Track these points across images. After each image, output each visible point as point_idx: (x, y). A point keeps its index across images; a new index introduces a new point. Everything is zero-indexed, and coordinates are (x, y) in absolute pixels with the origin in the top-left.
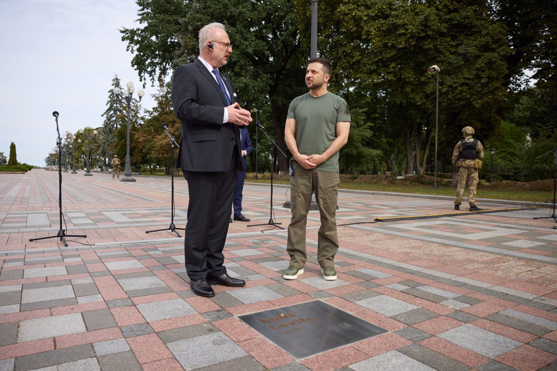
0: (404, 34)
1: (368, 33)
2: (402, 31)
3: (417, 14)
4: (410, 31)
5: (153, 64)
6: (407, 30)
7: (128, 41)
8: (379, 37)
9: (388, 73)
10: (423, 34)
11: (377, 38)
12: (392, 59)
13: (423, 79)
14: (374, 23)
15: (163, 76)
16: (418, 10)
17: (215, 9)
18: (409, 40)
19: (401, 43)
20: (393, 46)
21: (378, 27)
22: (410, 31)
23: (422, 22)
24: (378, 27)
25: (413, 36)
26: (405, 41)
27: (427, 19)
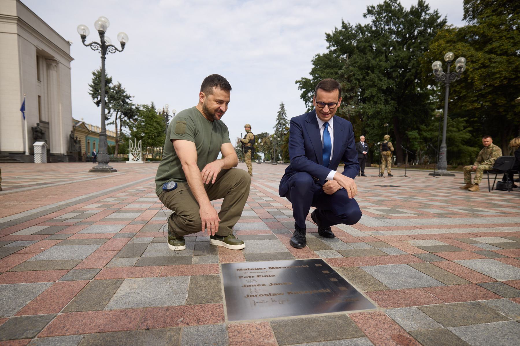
1: (473, 79)
2: (498, 76)
3: (510, 63)
6: (502, 74)
8: (480, 80)
9: (486, 101)
10: (513, 76)
11: (479, 81)
12: (489, 93)
13: (513, 103)
14: (477, 72)
16: (511, 61)
17: (361, 63)
19: (496, 83)
20: (491, 85)
21: (480, 74)
22: (504, 75)
23: (514, 69)
24: (480, 74)
25: (505, 78)
26: (500, 82)
27: (517, 67)
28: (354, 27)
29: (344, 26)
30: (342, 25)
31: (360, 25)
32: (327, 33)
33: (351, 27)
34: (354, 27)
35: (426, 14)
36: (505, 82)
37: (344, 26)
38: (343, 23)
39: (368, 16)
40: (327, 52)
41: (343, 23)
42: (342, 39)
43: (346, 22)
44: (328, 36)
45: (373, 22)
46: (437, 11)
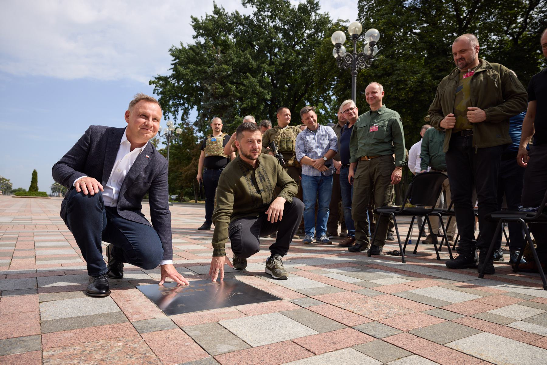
0: (404, 89)
4: (409, 86)
5: (176, 105)
6: (407, 85)
7: (155, 85)
15: (185, 116)
18: (408, 93)
22: (409, 86)
26: (405, 94)
28: (230, 14)
29: (217, 11)
30: (213, 9)
31: (237, 12)
32: (194, 17)
33: (226, 15)
34: (230, 14)
35: (316, 14)
36: (411, 95)
37: (217, 11)
38: (215, 7)
39: (247, 5)
40: (193, 42)
41: (215, 7)
42: (213, 27)
43: (219, 6)
44: (195, 20)
45: (255, 15)
46: (327, 14)
